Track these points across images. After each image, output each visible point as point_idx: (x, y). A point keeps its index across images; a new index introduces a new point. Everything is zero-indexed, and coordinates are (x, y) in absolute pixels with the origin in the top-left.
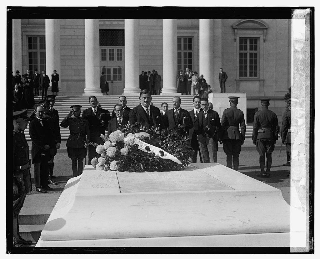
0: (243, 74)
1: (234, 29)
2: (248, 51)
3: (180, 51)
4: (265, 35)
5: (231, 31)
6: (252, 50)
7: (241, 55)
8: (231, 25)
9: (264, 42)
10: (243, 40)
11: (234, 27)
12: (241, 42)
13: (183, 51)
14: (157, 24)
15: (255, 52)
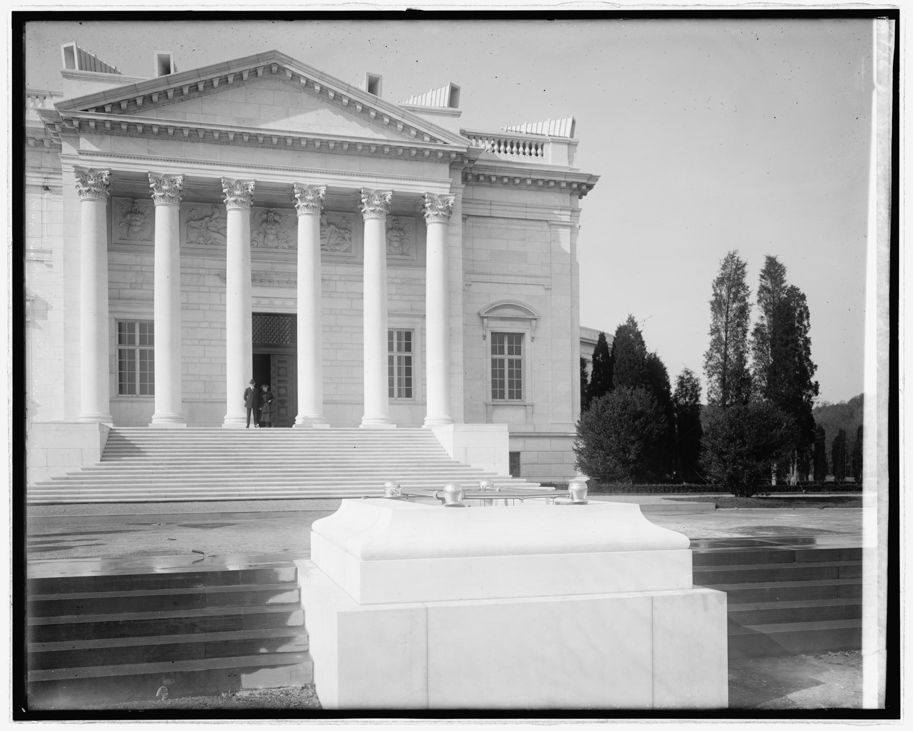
0: (497, 393)
1: (482, 318)
2: (506, 357)
3: (391, 354)
4: (534, 330)
5: (477, 321)
6: (513, 354)
7: (494, 361)
8: (477, 311)
9: (532, 341)
10: (497, 337)
11: (481, 315)
12: (493, 341)
13: (396, 354)
14: (351, 307)
15: (518, 357)
